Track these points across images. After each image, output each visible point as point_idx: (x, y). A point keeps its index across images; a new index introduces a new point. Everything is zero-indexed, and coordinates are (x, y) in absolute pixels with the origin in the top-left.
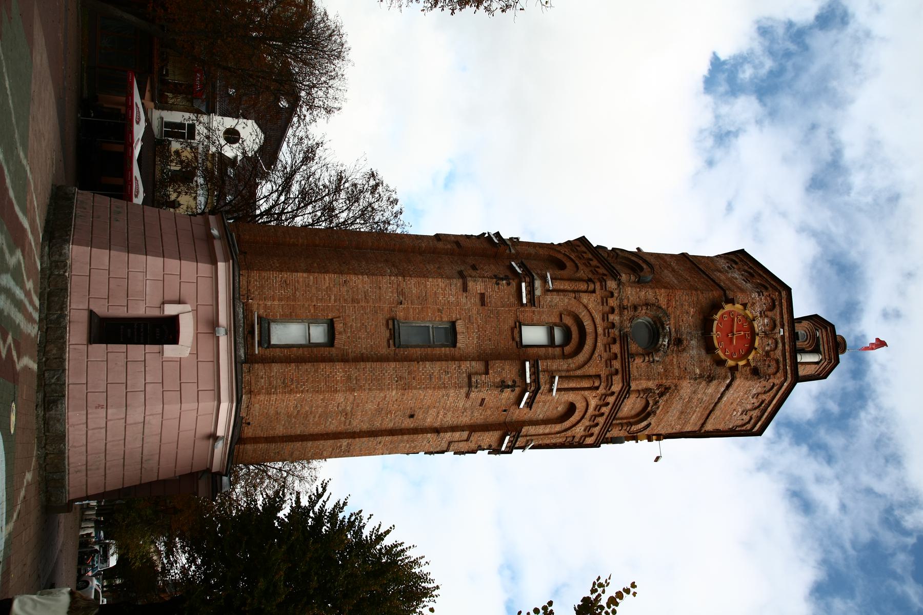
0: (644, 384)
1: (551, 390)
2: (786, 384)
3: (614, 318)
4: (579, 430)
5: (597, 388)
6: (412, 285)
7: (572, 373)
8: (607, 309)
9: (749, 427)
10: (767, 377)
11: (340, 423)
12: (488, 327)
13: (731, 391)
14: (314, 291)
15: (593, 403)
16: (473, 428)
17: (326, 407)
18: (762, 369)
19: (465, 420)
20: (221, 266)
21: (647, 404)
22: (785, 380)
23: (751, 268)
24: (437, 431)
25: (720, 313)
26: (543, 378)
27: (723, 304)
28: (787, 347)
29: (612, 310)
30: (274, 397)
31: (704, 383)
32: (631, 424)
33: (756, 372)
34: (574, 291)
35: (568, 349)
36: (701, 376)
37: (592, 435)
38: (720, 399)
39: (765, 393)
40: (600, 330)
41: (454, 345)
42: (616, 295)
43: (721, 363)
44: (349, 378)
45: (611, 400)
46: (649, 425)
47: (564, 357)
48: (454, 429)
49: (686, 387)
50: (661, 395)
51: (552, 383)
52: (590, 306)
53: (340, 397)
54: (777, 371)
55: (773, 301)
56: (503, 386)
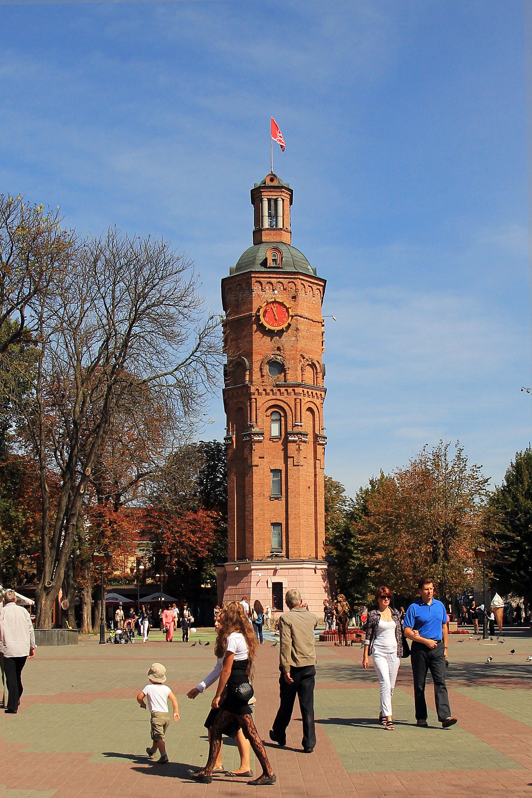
0: (300, 371)
1: (301, 426)
2: (301, 277)
3: (268, 389)
4: (318, 402)
5: (300, 399)
6: (256, 490)
7: (294, 414)
8: (264, 392)
9: (321, 288)
10: (296, 290)
11: (311, 518)
12: (273, 453)
13: (302, 314)
14: (260, 531)
15: (307, 399)
16: (315, 458)
17: (305, 526)
18: (293, 294)
19: (312, 461)
20: (252, 567)
21: (309, 365)
22: (299, 278)
23: (235, 282)
24: (315, 475)
25: (265, 324)
26: (296, 430)
27: (260, 323)
28: (281, 276)
29: (265, 390)
30: (302, 547)
31: (300, 334)
32: (317, 373)
33: (294, 297)
34: (256, 410)
35: (282, 414)
36: (296, 337)
37: (321, 395)
38: (306, 318)
39: (304, 287)
40: (274, 397)
41: (280, 471)
42: (258, 388)
43: (289, 325)
44: (295, 518)
45: (306, 390)
46: (318, 362)
47: (286, 416)
48: (315, 468)
49: (301, 345)
50: (304, 358)
51: (298, 425)
52: (263, 402)
53: (302, 521)
54: (294, 283)
55: (257, 282)
56: (299, 450)
